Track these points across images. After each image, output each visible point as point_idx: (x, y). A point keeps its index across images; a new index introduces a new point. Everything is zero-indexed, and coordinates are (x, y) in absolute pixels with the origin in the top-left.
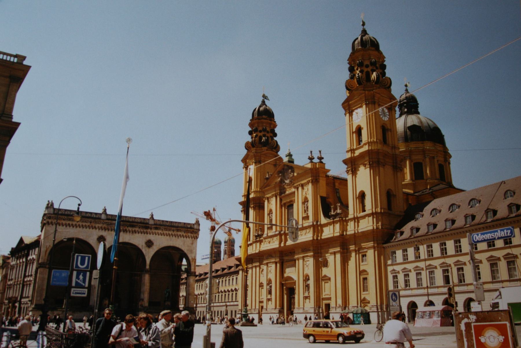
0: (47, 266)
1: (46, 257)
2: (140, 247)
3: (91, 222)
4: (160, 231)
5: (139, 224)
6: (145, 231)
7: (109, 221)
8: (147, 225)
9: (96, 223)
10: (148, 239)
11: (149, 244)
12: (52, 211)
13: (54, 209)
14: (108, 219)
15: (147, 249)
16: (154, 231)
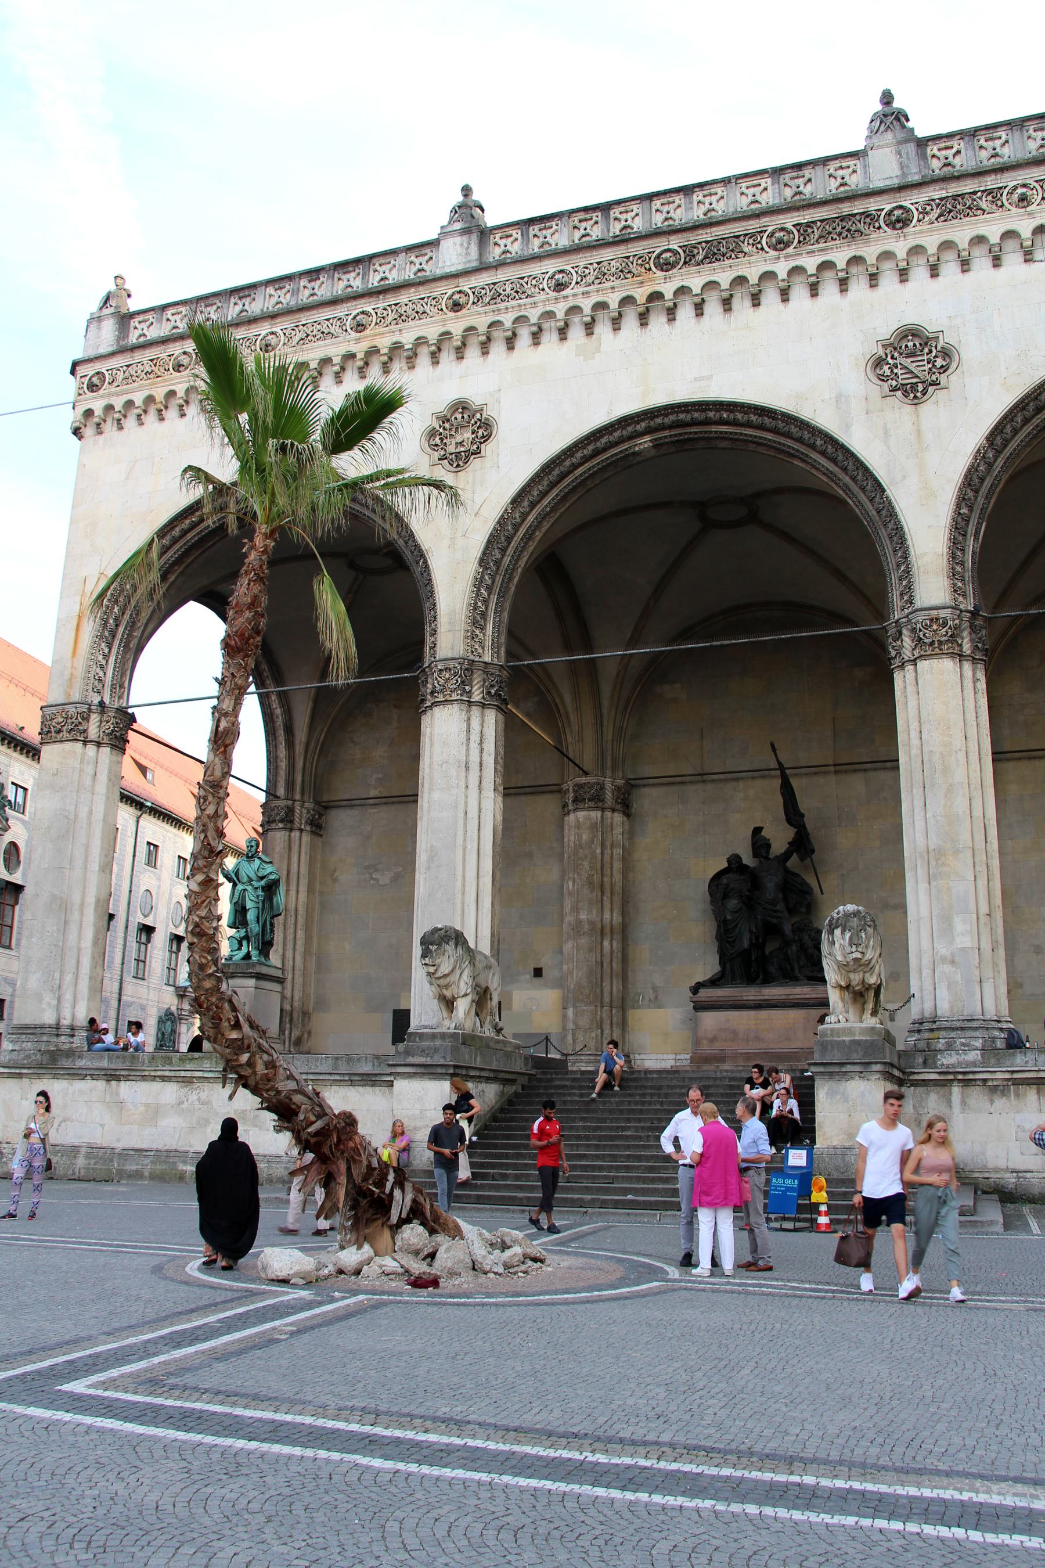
0: (93, 729)
1: (81, 663)
2: (825, 419)
3: (360, 327)
4: (992, 228)
5: (772, 223)
6: (840, 256)
7: (501, 275)
8: (858, 207)
9: (402, 318)
10: (886, 328)
11: (913, 364)
12: (107, 335)
13: (125, 319)
14: (483, 268)
15: (899, 411)
16: (929, 236)
